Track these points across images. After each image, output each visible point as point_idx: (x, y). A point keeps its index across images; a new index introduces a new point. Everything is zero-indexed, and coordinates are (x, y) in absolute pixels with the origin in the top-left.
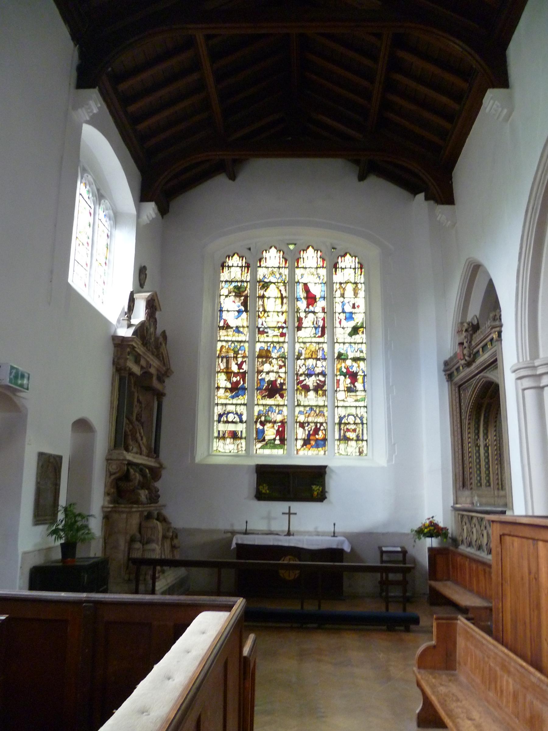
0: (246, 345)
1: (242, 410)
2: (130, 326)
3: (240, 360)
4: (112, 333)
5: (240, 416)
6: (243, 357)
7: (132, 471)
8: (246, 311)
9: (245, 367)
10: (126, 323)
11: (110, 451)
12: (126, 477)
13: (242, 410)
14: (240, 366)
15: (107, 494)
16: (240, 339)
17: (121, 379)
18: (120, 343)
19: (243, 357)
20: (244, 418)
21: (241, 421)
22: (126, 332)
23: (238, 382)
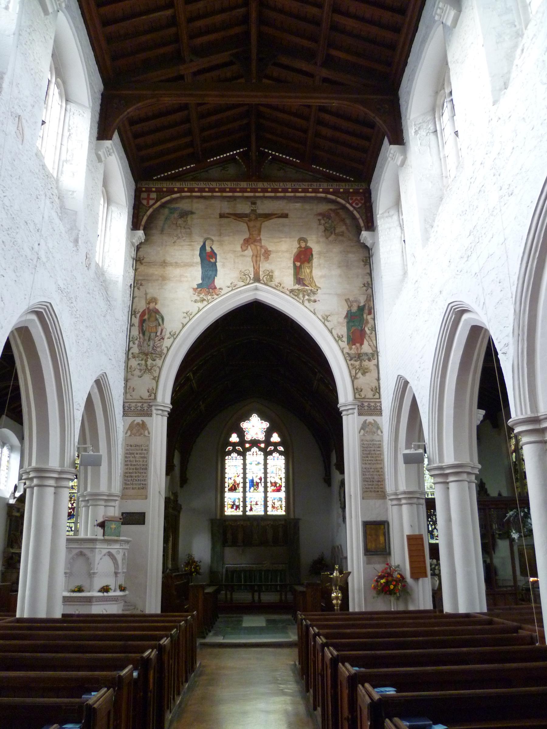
0: (76, 494)
1: (72, 525)
2: (15, 498)
3: (72, 502)
4: (6, 502)
5: (71, 528)
6: (74, 500)
7: (14, 556)
8: (77, 478)
9: (74, 505)
10: (13, 497)
11: (5, 549)
12: (11, 558)
13: (72, 525)
14: (72, 505)
15: (3, 565)
16: (73, 492)
17: (11, 520)
18: (10, 506)
19: (74, 500)
20: (73, 529)
21: (72, 531)
22: (12, 501)
23: (71, 512)
